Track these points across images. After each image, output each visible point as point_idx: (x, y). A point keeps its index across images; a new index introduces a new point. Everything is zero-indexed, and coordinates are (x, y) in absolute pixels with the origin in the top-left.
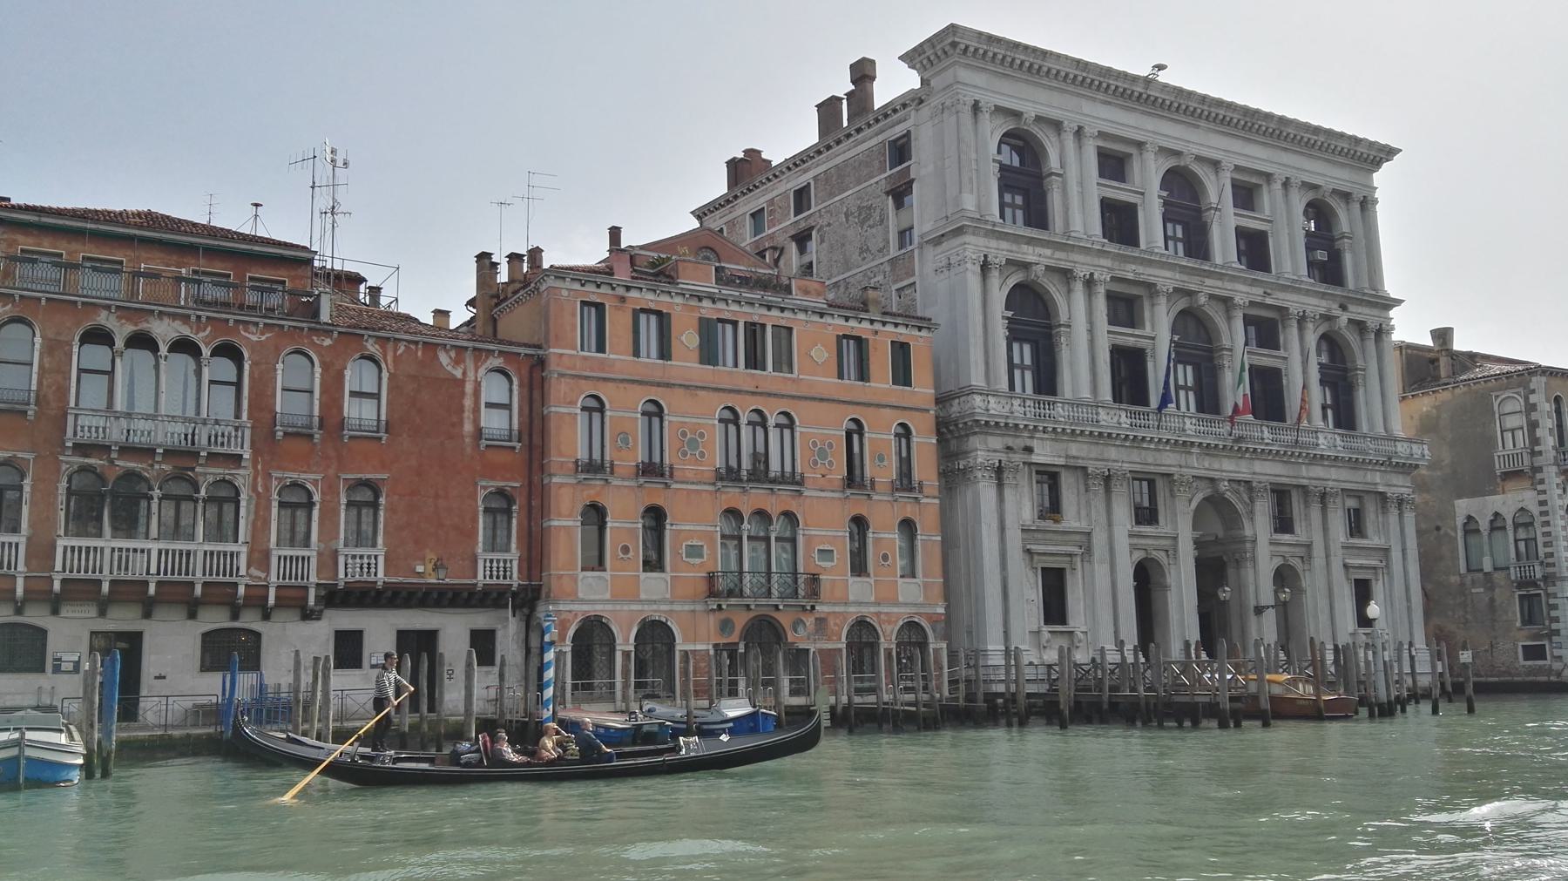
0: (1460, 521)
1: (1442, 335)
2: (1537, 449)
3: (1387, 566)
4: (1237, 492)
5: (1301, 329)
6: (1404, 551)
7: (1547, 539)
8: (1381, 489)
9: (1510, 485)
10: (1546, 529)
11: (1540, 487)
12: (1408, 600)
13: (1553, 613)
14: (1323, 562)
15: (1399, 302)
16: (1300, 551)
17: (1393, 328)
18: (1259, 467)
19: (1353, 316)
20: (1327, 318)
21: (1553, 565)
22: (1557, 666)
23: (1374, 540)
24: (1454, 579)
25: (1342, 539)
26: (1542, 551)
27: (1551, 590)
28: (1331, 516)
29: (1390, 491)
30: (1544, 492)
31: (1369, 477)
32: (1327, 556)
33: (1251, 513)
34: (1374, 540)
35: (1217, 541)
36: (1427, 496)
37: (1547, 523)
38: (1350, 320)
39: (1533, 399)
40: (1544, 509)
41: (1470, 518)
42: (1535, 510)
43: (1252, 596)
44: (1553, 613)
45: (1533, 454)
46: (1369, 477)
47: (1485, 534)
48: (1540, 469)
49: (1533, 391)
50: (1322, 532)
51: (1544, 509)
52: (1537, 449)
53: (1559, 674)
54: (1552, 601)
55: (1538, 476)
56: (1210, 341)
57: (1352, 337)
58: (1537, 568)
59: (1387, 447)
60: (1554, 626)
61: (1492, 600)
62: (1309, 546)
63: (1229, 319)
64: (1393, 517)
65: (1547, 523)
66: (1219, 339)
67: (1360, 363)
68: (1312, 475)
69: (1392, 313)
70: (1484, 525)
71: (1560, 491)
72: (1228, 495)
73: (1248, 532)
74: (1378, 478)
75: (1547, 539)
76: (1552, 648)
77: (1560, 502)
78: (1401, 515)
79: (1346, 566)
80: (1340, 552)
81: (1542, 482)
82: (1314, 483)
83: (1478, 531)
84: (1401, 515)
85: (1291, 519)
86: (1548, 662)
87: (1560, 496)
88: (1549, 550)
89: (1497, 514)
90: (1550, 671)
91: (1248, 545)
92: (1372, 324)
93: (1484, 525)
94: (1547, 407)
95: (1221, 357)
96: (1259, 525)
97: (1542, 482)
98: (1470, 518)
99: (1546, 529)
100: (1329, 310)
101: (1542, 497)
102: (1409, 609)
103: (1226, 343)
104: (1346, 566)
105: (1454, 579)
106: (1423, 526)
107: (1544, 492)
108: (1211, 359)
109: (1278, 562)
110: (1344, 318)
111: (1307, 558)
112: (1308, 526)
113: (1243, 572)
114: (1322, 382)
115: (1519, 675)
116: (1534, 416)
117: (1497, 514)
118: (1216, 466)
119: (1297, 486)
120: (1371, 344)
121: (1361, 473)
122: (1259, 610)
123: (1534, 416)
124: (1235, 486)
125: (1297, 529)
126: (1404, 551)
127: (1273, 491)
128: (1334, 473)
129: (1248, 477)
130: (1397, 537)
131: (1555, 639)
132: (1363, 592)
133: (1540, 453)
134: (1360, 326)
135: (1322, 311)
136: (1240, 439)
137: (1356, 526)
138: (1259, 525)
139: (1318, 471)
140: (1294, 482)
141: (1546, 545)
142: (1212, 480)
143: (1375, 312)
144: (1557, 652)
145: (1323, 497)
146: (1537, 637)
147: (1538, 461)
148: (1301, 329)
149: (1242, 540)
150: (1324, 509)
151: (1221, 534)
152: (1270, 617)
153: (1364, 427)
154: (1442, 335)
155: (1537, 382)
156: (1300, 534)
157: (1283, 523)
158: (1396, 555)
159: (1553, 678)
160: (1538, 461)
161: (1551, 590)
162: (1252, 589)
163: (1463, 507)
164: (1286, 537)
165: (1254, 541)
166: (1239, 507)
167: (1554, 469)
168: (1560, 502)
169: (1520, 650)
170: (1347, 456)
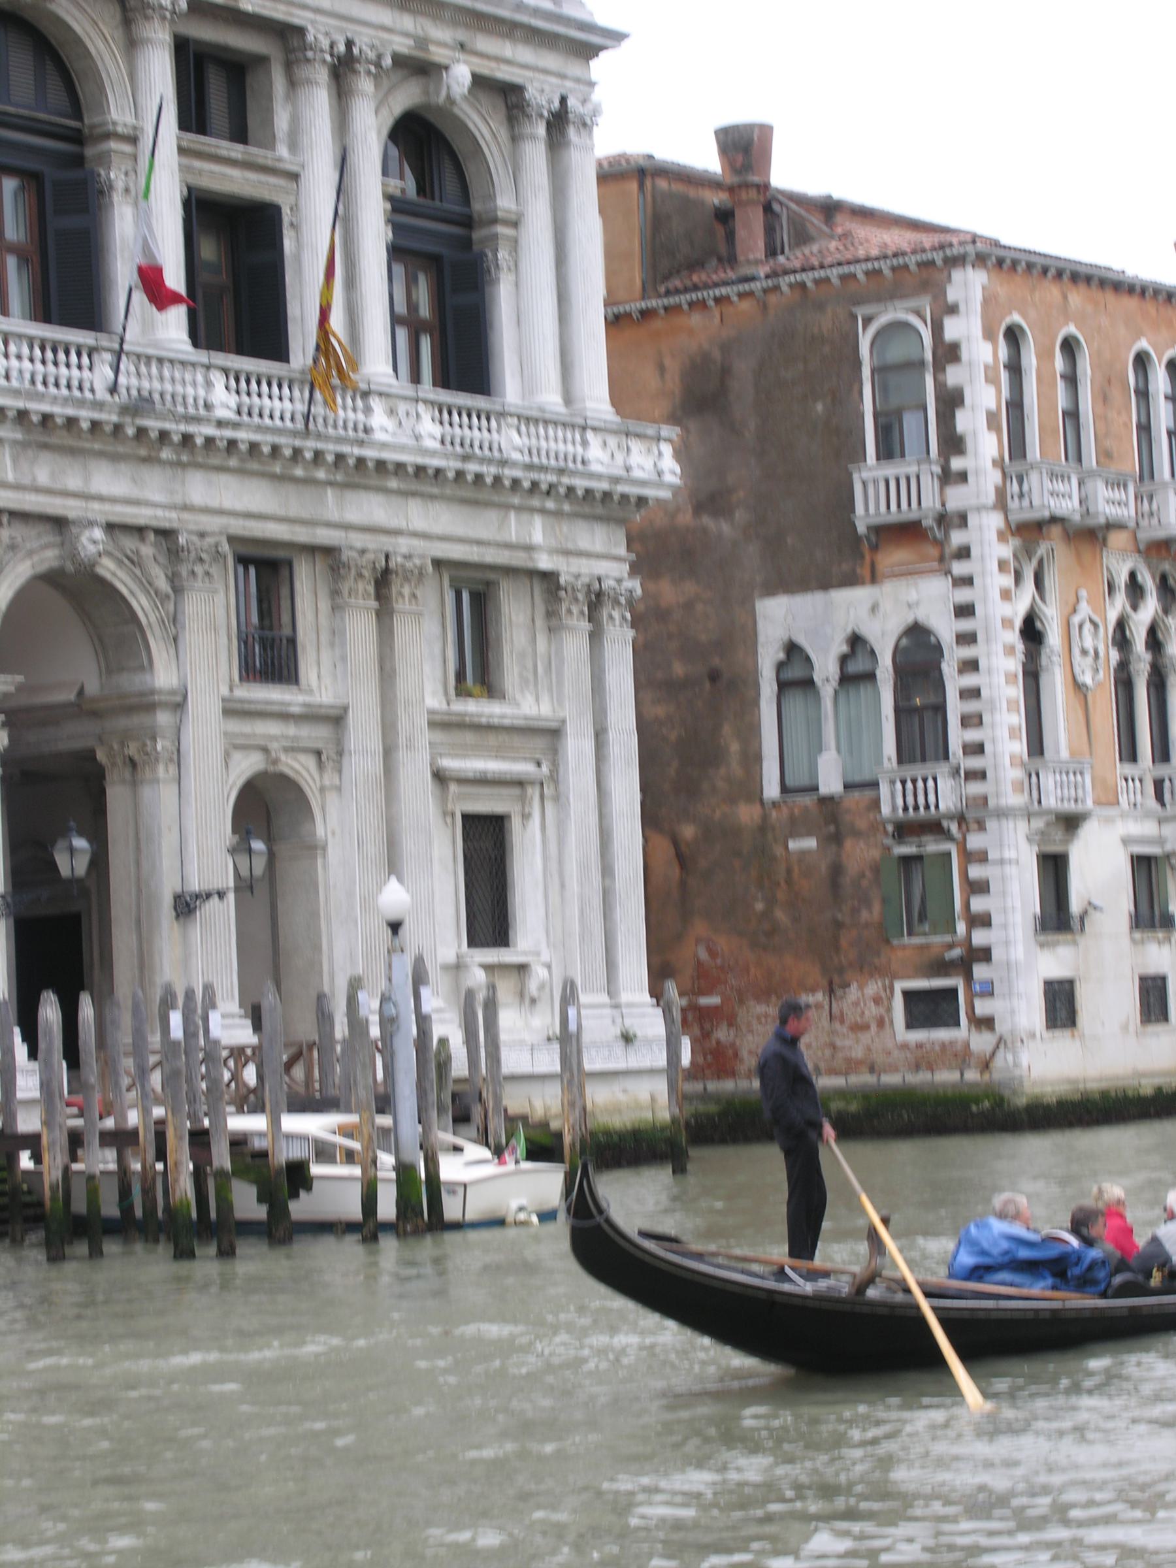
0: (768, 657)
1: (745, 147)
2: (956, 464)
3: (554, 777)
4: (134, 561)
5: (342, 92)
6: (600, 735)
7: (972, 706)
8: (544, 562)
9: (893, 557)
10: (969, 680)
11: (959, 568)
12: (607, 870)
13: (978, 904)
14: (376, 766)
15: (617, 37)
16: (317, 735)
17: (596, 112)
19: (487, 69)
20: (419, 68)
21: (980, 775)
22: (981, 1042)
23: (524, 704)
24: (747, 814)
25: (434, 700)
26: (957, 736)
27: (975, 841)
28: (403, 630)
30: (968, 581)
33: (174, 623)
34: (524, 704)
35: (83, 708)
36: (690, 588)
37: (971, 666)
38: (479, 82)
39: (952, 329)
40: (965, 625)
41: (792, 649)
42: (945, 628)
43: (167, 863)
44: (978, 904)
45: (948, 477)
47: (827, 691)
48: (962, 520)
49: (953, 310)
50: (374, 675)
51: (965, 625)
52: (956, 464)
53: (986, 1065)
54: (975, 872)
55: (957, 538)
56: (78, 114)
57: (484, 125)
58: (946, 785)
59: (557, 445)
60: (980, 938)
61: (837, 870)
62: (336, 719)
63: (132, 44)
64: (575, 644)
65: (971, 666)
66: (101, 105)
67: (505, 203)
68: (353, 515)
69: (599, 67)
70: (826, 669)
71: (1008, 581)
72: (108, 568)
73: (164, 677)
74: (537, 531)
75: (972, 706)
76: (971, 997)
77: (1006, 609)
78: (596, 637)
79: (440, 777)
80: (424, 737)
81: (964, 553)
82: (359, 540)
83: (808, 684)
84: (596, 637)
85: (292, 641)
86: (962, 1032)
87: (1006, 595)
88: (972, 735)
89: (856, 641)
90: (962, 1056)
91: (163, 718)
92: (541, 94)
93: (826, 669)
94: (982, 355)
95: (105, 159)
96: (195, 657)
97: (964, 553)
98: (792, 649)
99: (969, 680)
100: (422, 42)
101: (963, 595)
102: (607, 895)
103: (119, 114)
104: (440, 777)
105: (747, 814)
106: (679, 669)
107: (968, 581)
108: (78, 161)
109: (247, 765)
110: (460, 75)
111: (330, 757)
112: (335, 660)
113: (146, 792)
114: (396, 252)
115: (894, 1069)
116: (953, 376)
117: (856, 641)
118: (73, 482)
119: (312, 550)
120: (535, 154)
121: (492, 515)
122: (185, 906)
123: (953, 376)
124: (129, 543)
125: (308, 670)
126: (600, 735)
127: (243, 561)
130: (582, 696)
131: (980, 971)
132: (486, 850)
133: (963, 477)
134: (508, 97)
135: (403, 45)
136: (141, 405)
137: (478, 668)
138: (195, 657)
140: (302, 535)
141: (969, 721)
142: (59, 523)
143: (550, 60)
144: (982, 1007)
146: (941, 967)
147: (957, 498)
148: (342, 92)
149: (146, 704)
151: (93, 687)
152: (221, 920)
153: (511, 389)
154: (745, 147)
155: (969, 286)
156: (320, 680)
159: (972, 1075)
160: (957, 498)
161: (975, 841)
162: (168, 843)
163: (779, 618)
165: (179, 705)
166: (141, 604)
167: (995, 521)
168: (1006, 609)
169: (898, 1003)
170: (451, 465)
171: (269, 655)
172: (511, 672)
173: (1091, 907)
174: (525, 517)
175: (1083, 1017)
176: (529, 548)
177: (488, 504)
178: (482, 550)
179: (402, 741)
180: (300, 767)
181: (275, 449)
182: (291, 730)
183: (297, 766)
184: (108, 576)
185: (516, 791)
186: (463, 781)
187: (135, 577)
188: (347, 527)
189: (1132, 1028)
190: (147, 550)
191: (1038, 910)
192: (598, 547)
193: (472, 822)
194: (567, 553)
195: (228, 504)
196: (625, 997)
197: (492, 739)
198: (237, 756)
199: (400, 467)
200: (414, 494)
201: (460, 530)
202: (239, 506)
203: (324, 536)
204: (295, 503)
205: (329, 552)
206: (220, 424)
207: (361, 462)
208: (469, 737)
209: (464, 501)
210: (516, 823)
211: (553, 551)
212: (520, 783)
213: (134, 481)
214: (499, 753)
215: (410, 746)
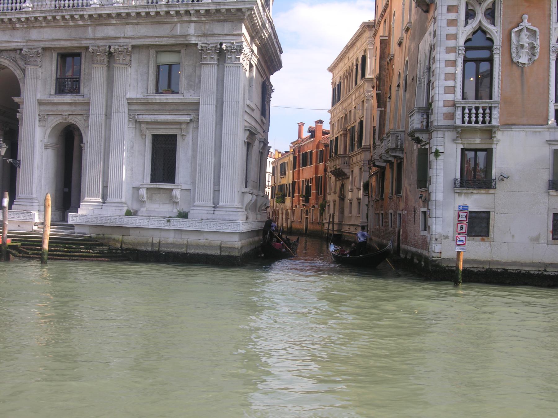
8: (193, 41)
18: (35, 34)
29: (201, 42)
31: (179, 29)
32: (108, 116)
34: (188, 95)
46: (179, 29)
68: (99, 35)
74: (192, 29)
82: (100, 43)
121: (168, 26)
124: (13, 54)
125: (83, 89)
128: (129, 31)
129: (20, 45)
139: (110, 31)
140: (75, 44)
145: (110, 55)
150: (110, 67)
157: (68, 84)
158: (207, 110)
164: (68, 98)
166: (18, 73)
171: (68, 84)
172: (183, 83)
173: (503, 178)
174: (186, 25)
175: (491, 233)
176: (185, 36)
177: (165, 23)
178: (161, 39)
179: (114, 109)
180: (78, 121)
181: (54, 18)
182: (73, 108)
183: (77, 120)
184: (7, 65)
185: (178, 126)
186: (147, 123)
187: (15, 65)
188: (94, 39)
189: (543, 240)
190: (18, 56)
191: (458, 176)
192: (225, 32)
193: (155, 138)
194: (205, 35)
195: (46, 38)
196: (221, 204)
197: (168, 107)
198: (51, 118)
199: (109, 15)
200: (127, 24)
201: (150, 33)
202: (50, 38)
203: (85, 43)
204: (74, 33)
205: (87, 48)
206: (26, 12)
207: (91, 16)
208: (156, 107)
209: (152, 23)
210: (179, 139)
211: (199, 36)
212: (180, 123)
213: (10, 35)
214: (169, 113)
215: (118, 111)
